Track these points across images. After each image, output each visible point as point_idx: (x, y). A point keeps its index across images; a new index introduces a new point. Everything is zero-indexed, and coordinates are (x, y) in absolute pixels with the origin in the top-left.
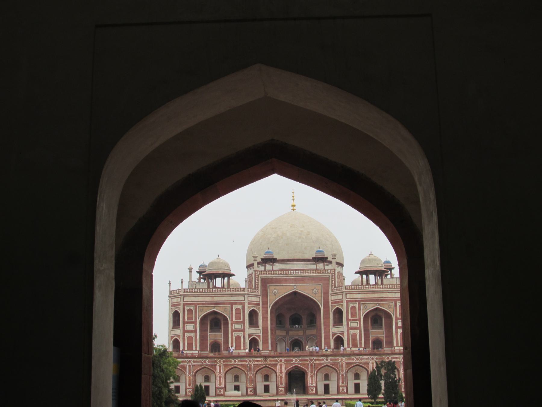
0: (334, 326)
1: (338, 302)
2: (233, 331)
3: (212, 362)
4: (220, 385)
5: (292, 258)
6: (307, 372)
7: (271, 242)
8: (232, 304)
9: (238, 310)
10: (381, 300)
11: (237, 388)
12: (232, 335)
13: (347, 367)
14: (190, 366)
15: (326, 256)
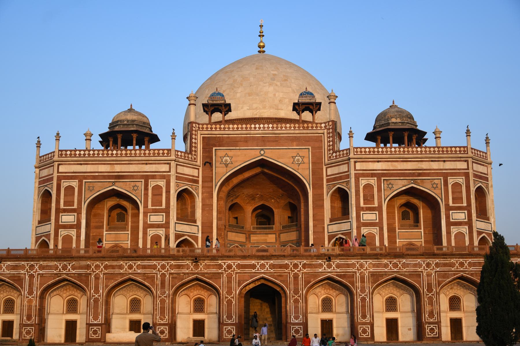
0: (331, 220)
1: (340, 178)
2: (147, 226)
3: (81, 268)
4: (96, 318)
5: (257, 116)
6: (285, 292)
7: (224, 91)
8: (147, 178)
9: (157, 188)
10: (420, 175)
11: (134, 326)
12: (145, 233)
13: (374, 283)
14: (31, 276)
15: (317, 101)
